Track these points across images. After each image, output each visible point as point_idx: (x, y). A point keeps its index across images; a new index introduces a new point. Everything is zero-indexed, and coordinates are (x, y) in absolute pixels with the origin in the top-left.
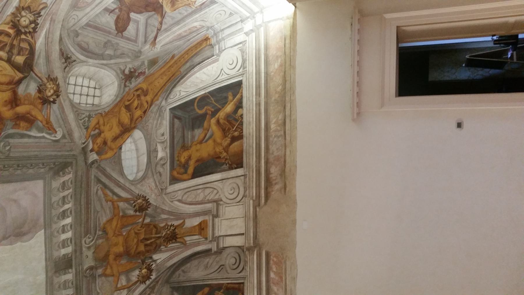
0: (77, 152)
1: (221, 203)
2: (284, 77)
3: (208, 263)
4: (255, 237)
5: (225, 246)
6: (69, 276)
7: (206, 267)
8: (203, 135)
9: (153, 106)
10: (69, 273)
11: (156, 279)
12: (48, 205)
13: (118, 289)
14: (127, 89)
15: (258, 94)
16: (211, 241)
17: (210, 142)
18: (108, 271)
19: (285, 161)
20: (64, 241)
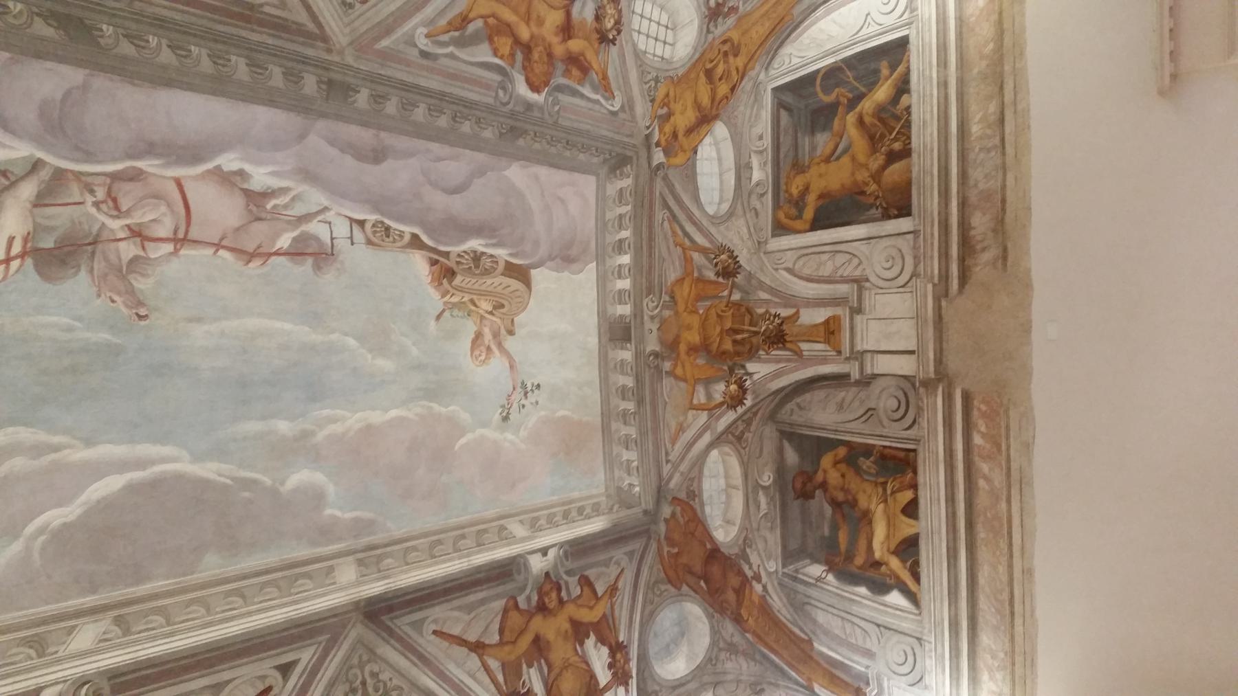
0: (638, 140)
1: (867, 285)
2: (1000, 22)
3: (843, 399)
4: (939, 361)
5: (876, 372)
6: (627, 355)
7: (840, 407)
8: (831, 146)
9: (746, 79)
11: (753, 406)
12: (602, 226)
13: (693, 407)
14: (710, 37)
15: (943, 63)
16: (847, 359)
17: (846, 160)
19: (1004, 201)
20: (620, 292)
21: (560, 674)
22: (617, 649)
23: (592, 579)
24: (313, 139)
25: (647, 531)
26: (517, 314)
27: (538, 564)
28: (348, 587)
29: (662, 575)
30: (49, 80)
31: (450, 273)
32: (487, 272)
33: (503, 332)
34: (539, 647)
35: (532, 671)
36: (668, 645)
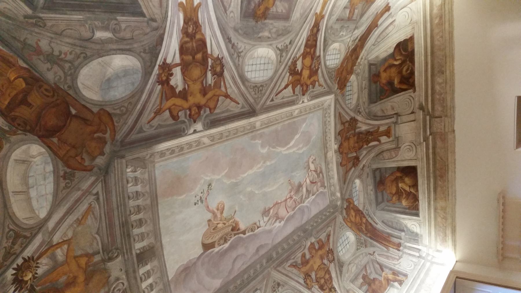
6: (138, 246)
10: (139, 249)
18: (83, 261)
20: (149, 277)
21: (199, 78)
22: (164, 81)
23: (171, 119)
24: (270, 242)
25: (122, 146)
26: (208, 229)
27: (199, 126)
28: (258, 120)
29: (115, 119)
30: (305, 219)
31: (233, 230)
32: (221, 238)
33: (212, 219)
34: (204, 91)
35: (210, 83)
36: (124, 76)
